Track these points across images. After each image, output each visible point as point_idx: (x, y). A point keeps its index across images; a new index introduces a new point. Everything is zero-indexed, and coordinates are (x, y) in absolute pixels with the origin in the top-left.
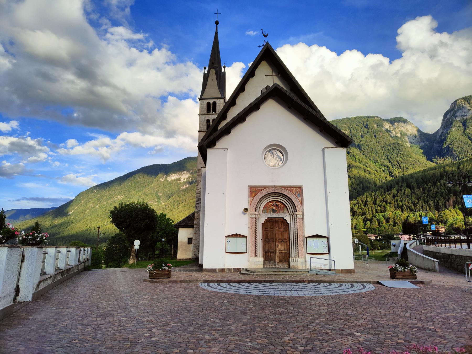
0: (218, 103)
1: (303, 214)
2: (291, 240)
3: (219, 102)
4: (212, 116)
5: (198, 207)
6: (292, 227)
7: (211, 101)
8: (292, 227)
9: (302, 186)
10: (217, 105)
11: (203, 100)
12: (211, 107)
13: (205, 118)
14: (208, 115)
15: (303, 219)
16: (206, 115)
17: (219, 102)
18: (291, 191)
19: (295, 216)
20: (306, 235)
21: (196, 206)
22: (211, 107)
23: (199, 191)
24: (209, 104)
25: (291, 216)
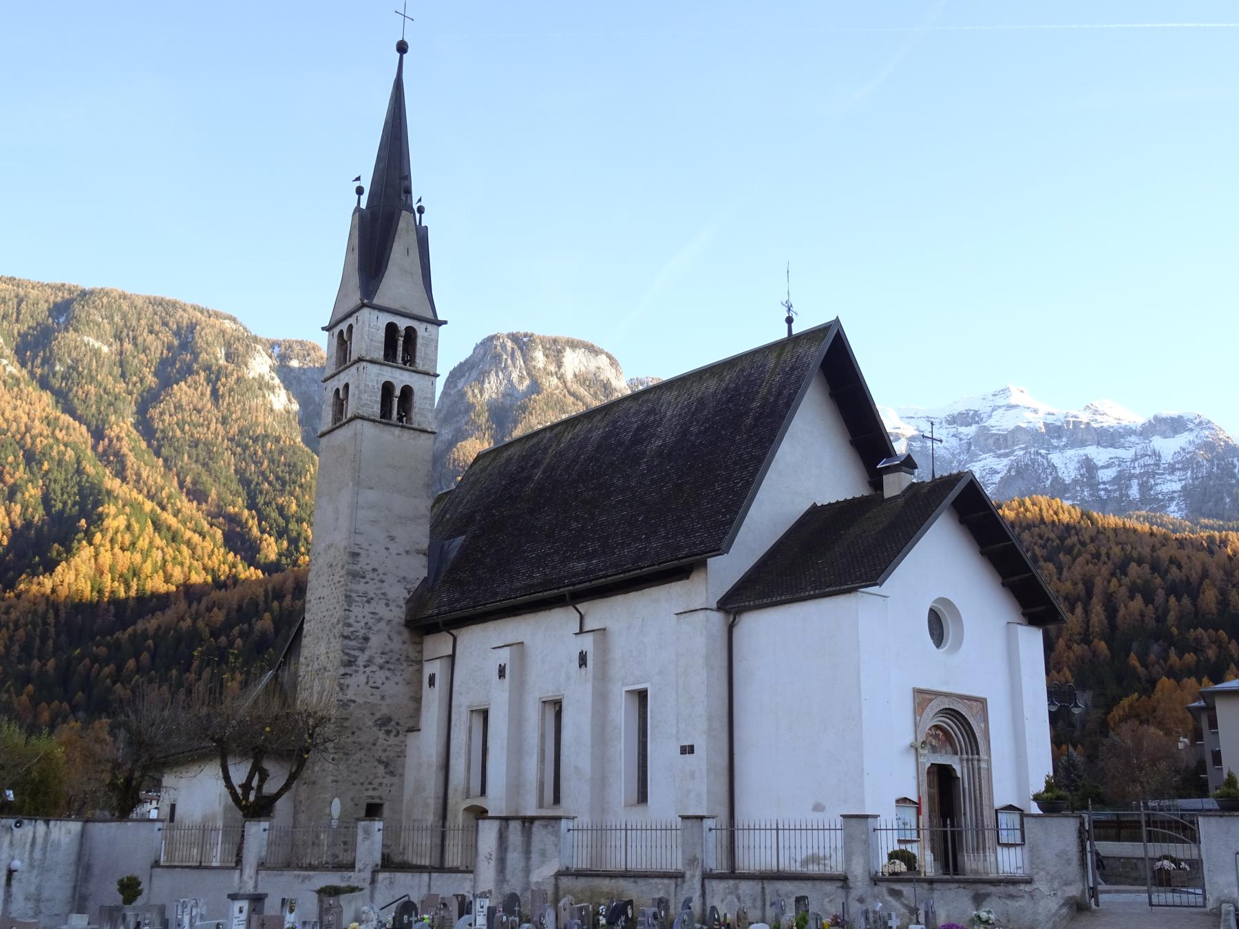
0: (423, 338)
1: (989, 761)
2: (965, 814)
3: (426, 334)
4: (401, 375)
5: (348, 686)
6: (966, 785)
7: (402, 323)
8: (966, 785)
9: (986, 700)
10: (419, 341)
11: (376, 312)
12: (401, 341)
13: (378, 375)
14: (389, 369)
15: (989, 770)
16: (385, 368)
17: (426, 334)
18: (971, 707)
19: (976, 763)
20: (998, 804)
21: (342, 681)
22: (401, 341)
23: (351, 629)
24: (391, 329)
25: (965, 763)
